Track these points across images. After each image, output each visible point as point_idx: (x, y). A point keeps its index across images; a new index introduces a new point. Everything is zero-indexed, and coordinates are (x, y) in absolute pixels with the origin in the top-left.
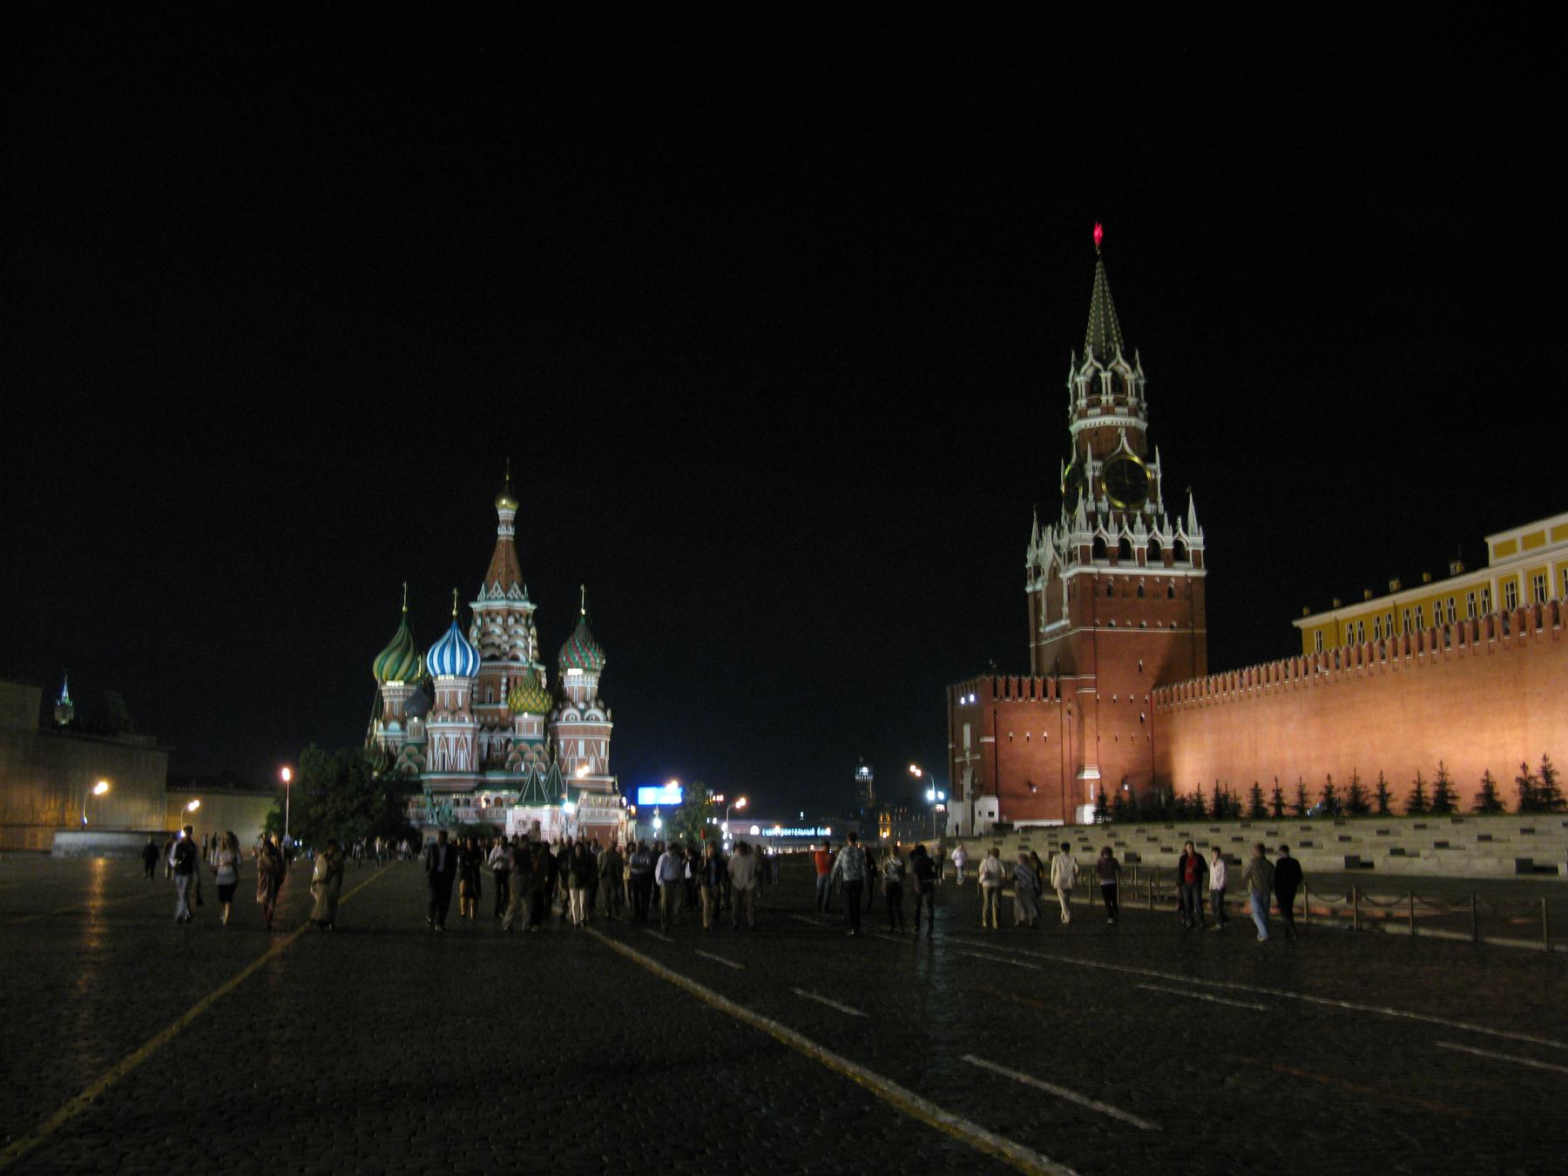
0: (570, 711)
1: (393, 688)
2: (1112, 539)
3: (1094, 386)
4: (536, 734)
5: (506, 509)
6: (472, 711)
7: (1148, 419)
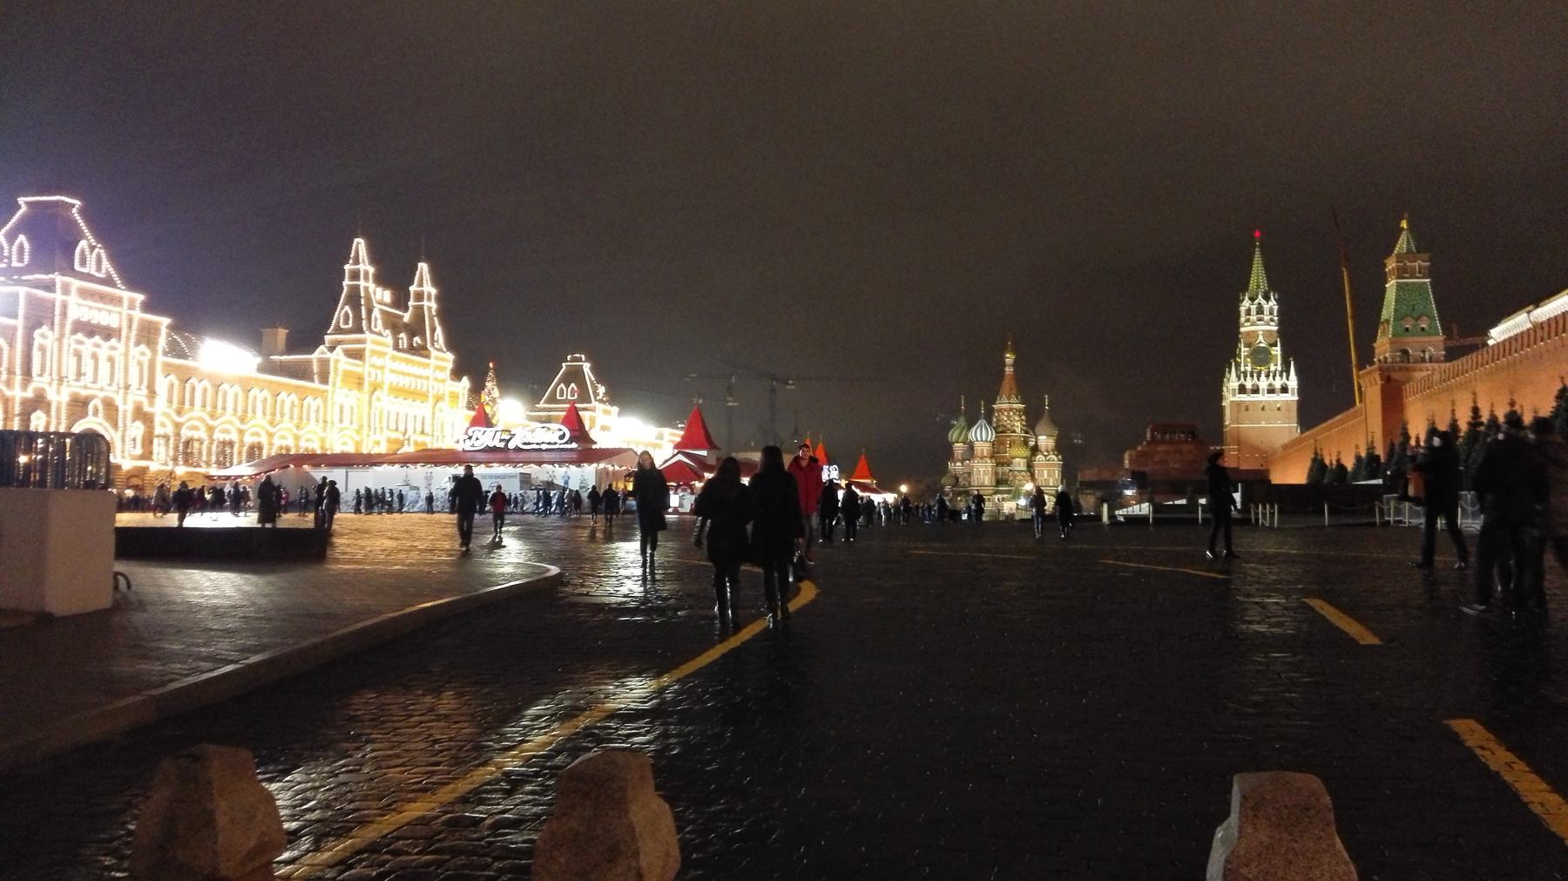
0: (1039, 457)
1: (959, 447)
2: (1249, 385)
3: (1248, 312)
4: (1023, 467)
5: (1009, 358)
6: (991, 457)
7: (1280, 324)
